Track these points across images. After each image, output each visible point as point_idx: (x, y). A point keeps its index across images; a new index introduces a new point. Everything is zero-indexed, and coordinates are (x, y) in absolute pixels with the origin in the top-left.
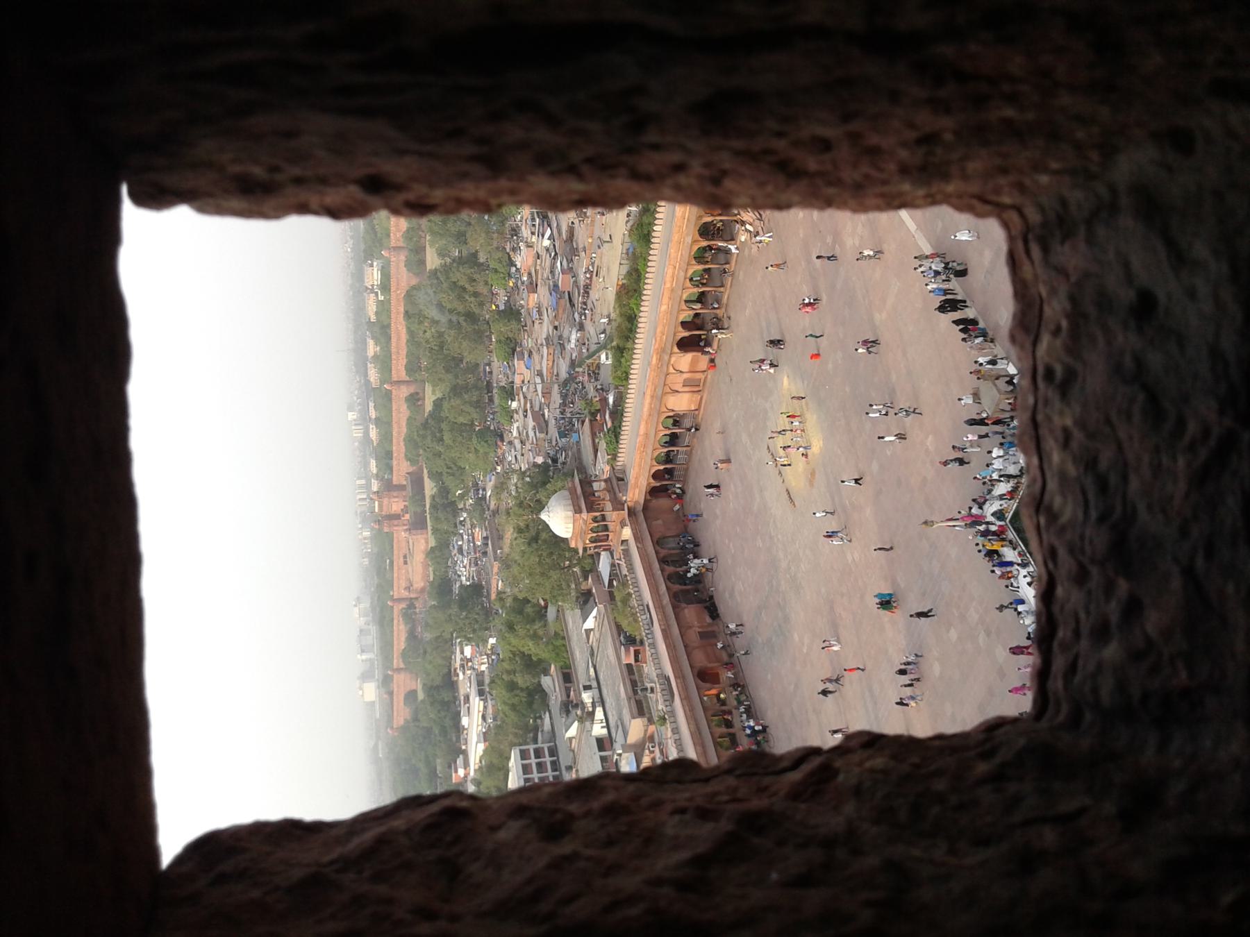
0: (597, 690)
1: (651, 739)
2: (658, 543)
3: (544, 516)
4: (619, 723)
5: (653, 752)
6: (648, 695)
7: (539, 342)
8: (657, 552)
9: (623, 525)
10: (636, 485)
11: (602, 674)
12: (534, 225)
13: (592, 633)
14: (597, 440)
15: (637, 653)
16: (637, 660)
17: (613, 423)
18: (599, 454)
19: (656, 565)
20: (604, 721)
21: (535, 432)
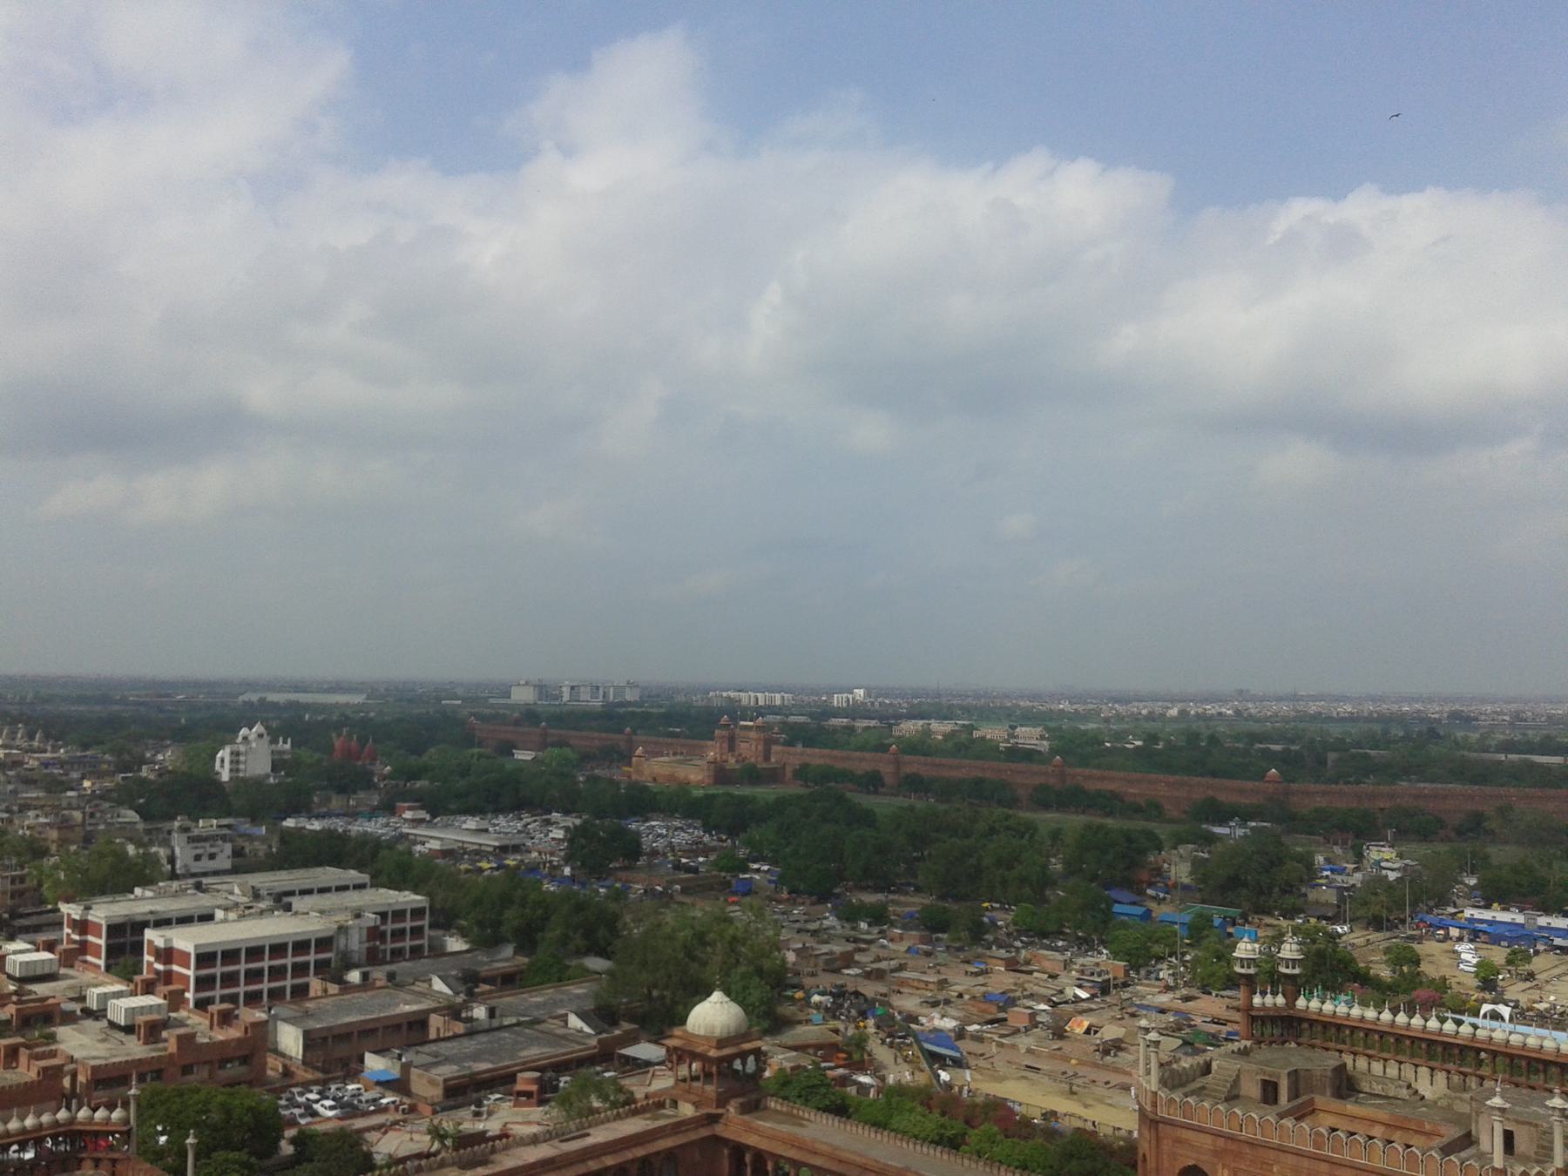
0: (487, 1027)
1: (413, 1109)
2: (670, 1154)
3: (717, 996)
4: (440, 1059)
5: (397, 1109)
6: (473, 1108)
7: (943, 969)
8: (658, 1153)
9: (696, 1105)
10: (750, 1130)
11: (507, 1035)
12: (1092, 974)
13: (562, 1024)
14: (811, 1051)
15: (528, 1095)
16: (520, 1094)
17: (833, 1079)
18: (794, 1054)
19: (640, 1152)
20: (447, 1035)
21: (826, 954)
